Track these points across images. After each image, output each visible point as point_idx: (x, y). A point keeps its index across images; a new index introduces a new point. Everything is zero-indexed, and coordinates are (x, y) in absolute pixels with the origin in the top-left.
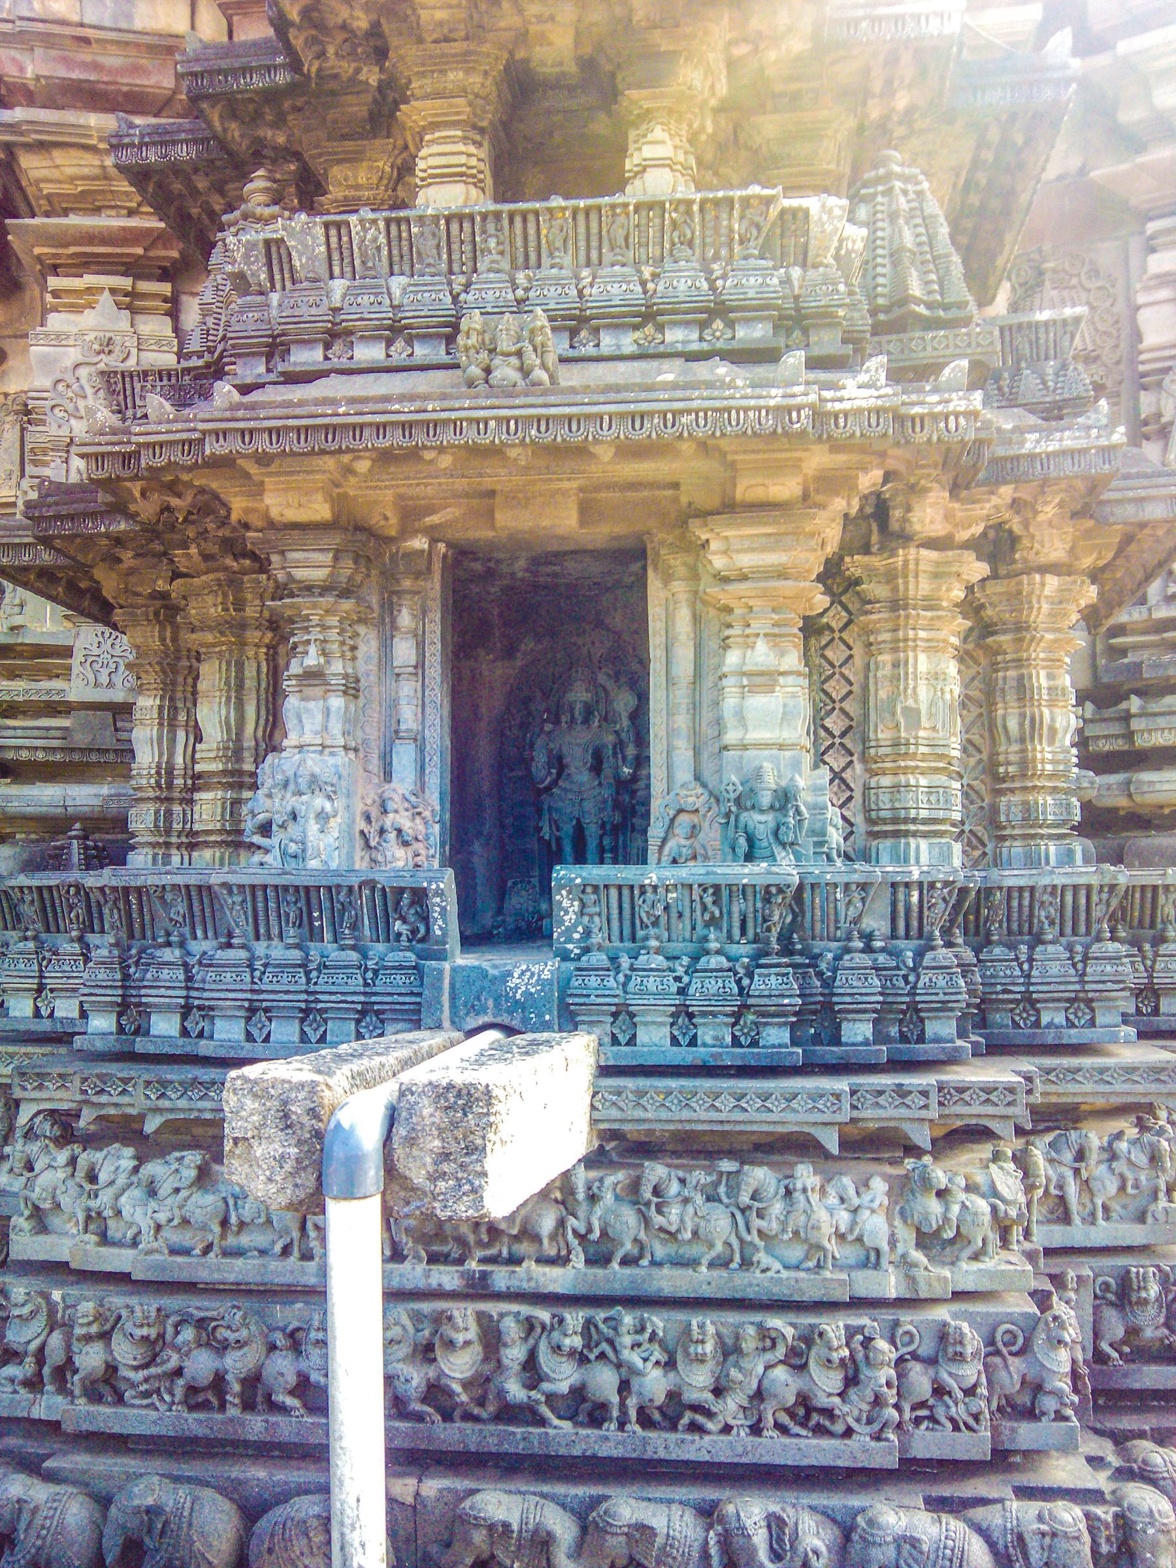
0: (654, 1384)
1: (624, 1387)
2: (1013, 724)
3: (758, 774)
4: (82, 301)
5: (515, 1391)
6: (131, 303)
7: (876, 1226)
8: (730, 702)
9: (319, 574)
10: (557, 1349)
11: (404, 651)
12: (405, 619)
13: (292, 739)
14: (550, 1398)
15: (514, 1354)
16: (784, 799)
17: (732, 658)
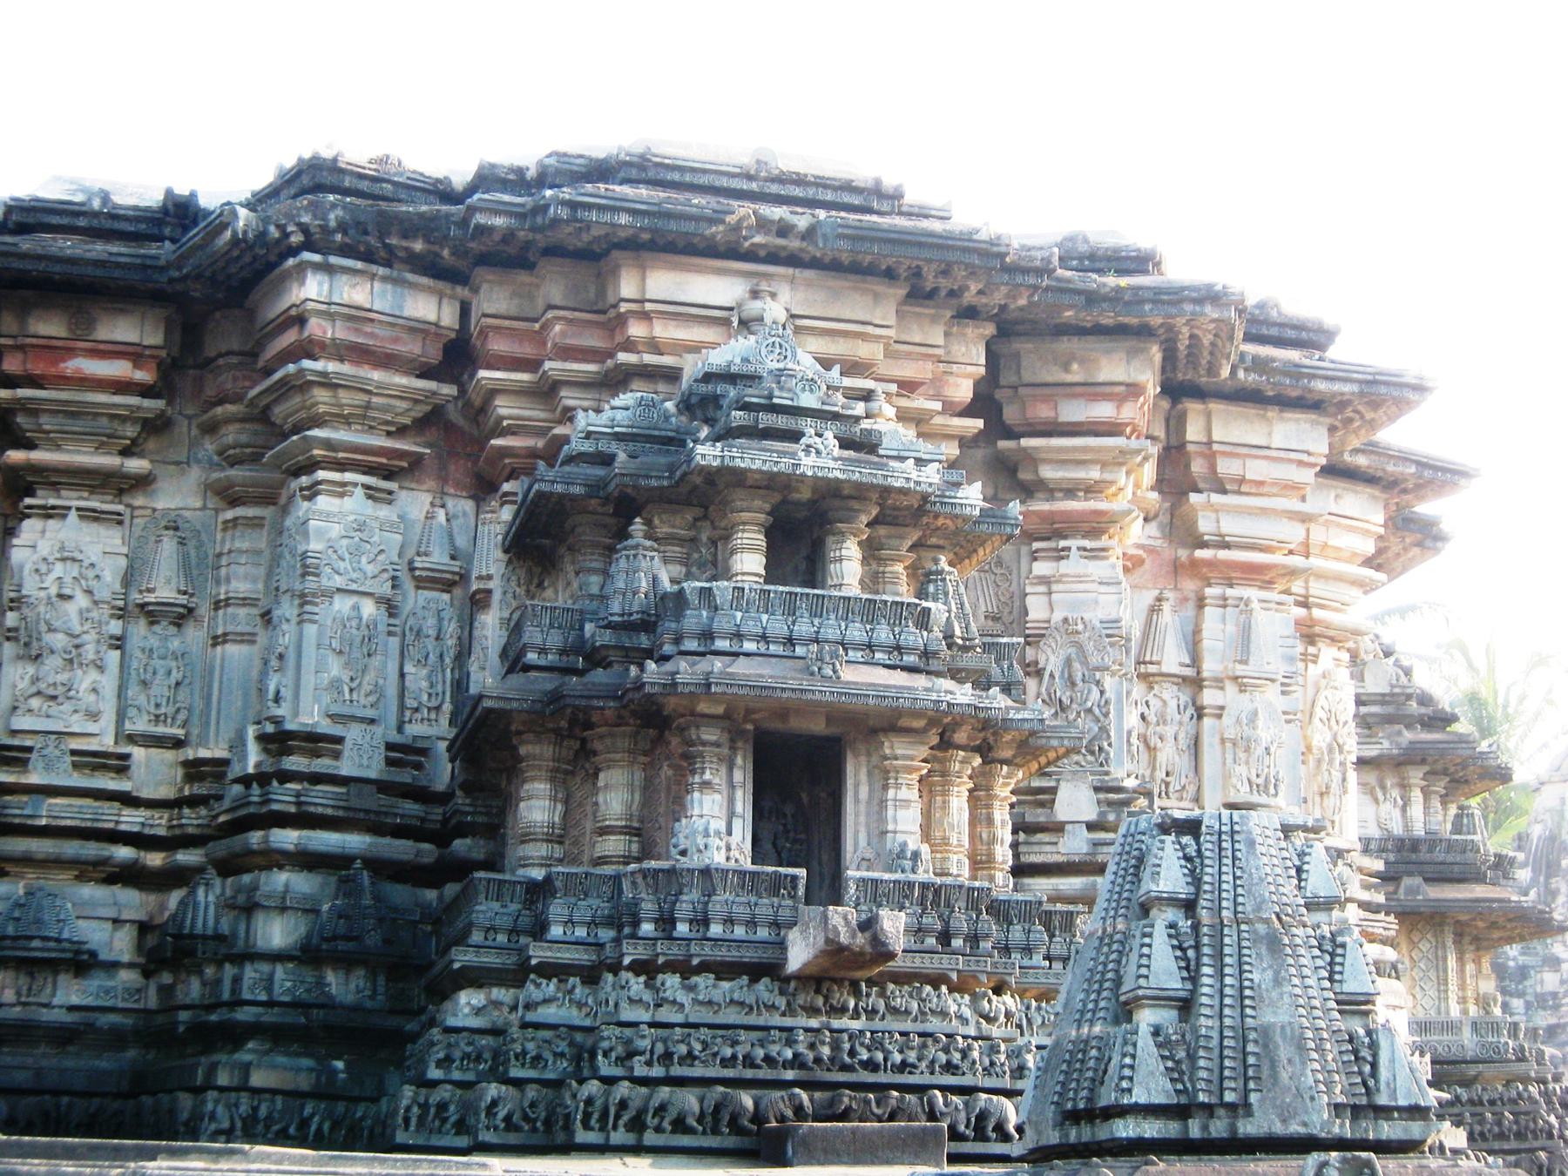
0: (897, 1058)
1: (885, 1060)
2: (984, 836)
3: (905, 844)
4: (342, 490)
5: (847, 1059)
6: (372, 493)
7: (967, 1012)
8: (890, 812)
9: (714, 738)
10: (862, 1044)
11: (738, 776)
12: (739, 761)
13: (696, 812)
14: (861, 1063)
15: (847, 1046)
16: (916, 855)
17: (891, 793)
